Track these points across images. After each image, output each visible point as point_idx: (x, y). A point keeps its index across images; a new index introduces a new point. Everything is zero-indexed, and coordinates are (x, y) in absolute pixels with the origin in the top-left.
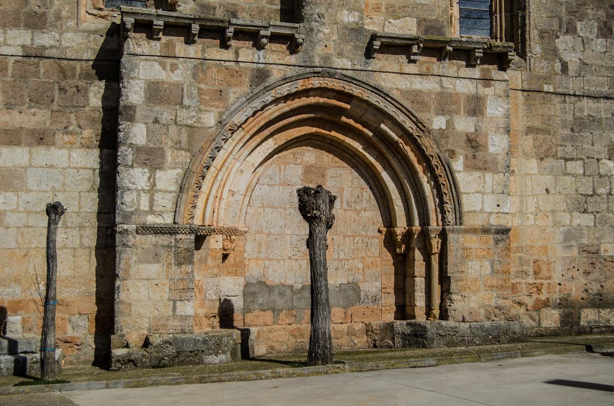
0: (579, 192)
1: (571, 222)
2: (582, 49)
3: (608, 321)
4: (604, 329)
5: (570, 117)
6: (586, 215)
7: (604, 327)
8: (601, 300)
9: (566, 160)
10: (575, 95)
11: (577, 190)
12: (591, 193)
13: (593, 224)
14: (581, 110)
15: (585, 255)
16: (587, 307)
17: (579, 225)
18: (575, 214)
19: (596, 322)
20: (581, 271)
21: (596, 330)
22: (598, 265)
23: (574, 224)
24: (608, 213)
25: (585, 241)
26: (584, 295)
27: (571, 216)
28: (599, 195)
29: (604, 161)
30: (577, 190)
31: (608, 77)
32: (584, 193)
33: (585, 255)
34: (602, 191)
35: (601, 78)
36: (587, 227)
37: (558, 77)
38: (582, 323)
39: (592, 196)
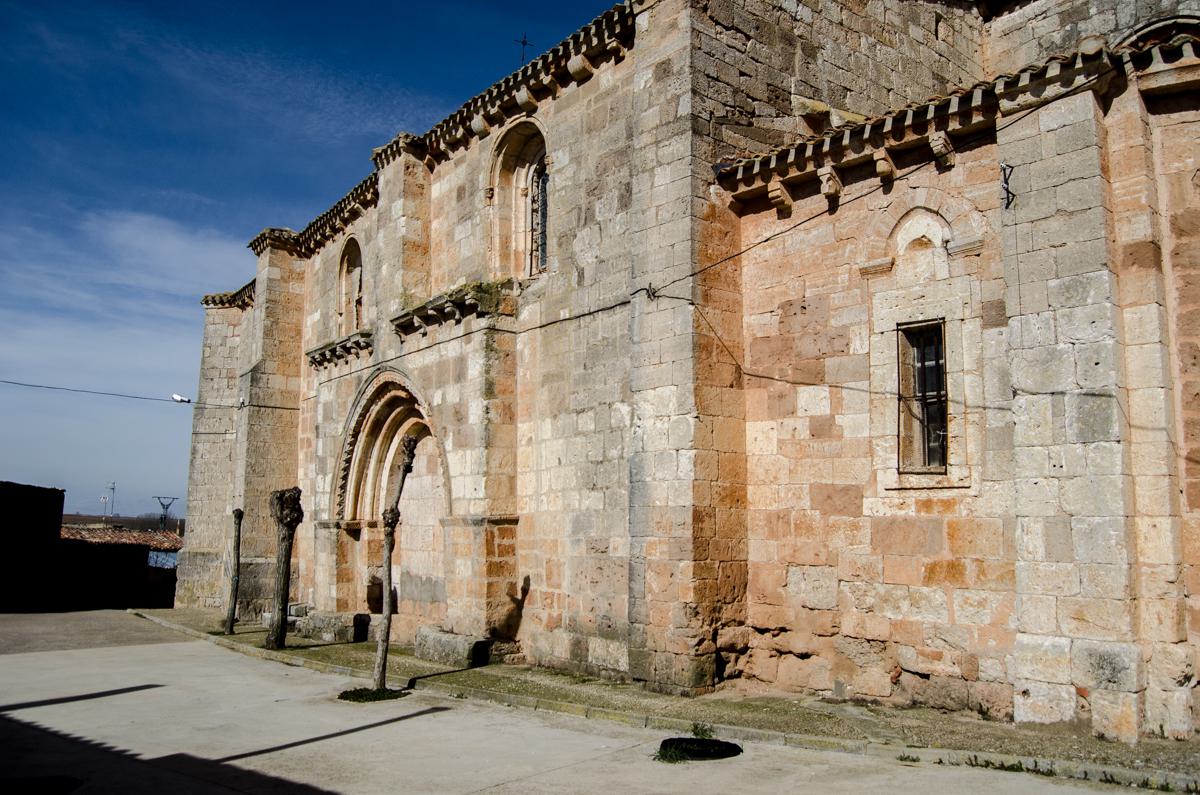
0: (590, 459)
1: (580, 505)
2: (599, 240)
3: (617, 661)
4: (612, 674)
5: (583, 349)
6: (594, 494)
7: (614, 670)
8: (609, 626)
9: (578, 413)
10: (590, 314)
11: (587, 456)
12: (601, 459)
13: (601, 507)
14: (595, 334)
15: (593, 555)
16: (594, 635)
17: (588, 509)
18: (585, 492)
19: (604, 661)
20: (589, 580)
21: (603, 672)
22: (606, 571)
23: (584, 507)
24: (619, 488)
25: (593, 534)
26: (591, 616)
27: (580, 495)
28: (610, 461)
29: (618, 405)
30: (587, 456)
31: (626, 269)
32: (593, 459)
33: (593, 555)
34: (614, 453)
35: (618, 275)
36: (595, 510)
37: (574, 293)
38: (590, 659)
39: (601, 462)
